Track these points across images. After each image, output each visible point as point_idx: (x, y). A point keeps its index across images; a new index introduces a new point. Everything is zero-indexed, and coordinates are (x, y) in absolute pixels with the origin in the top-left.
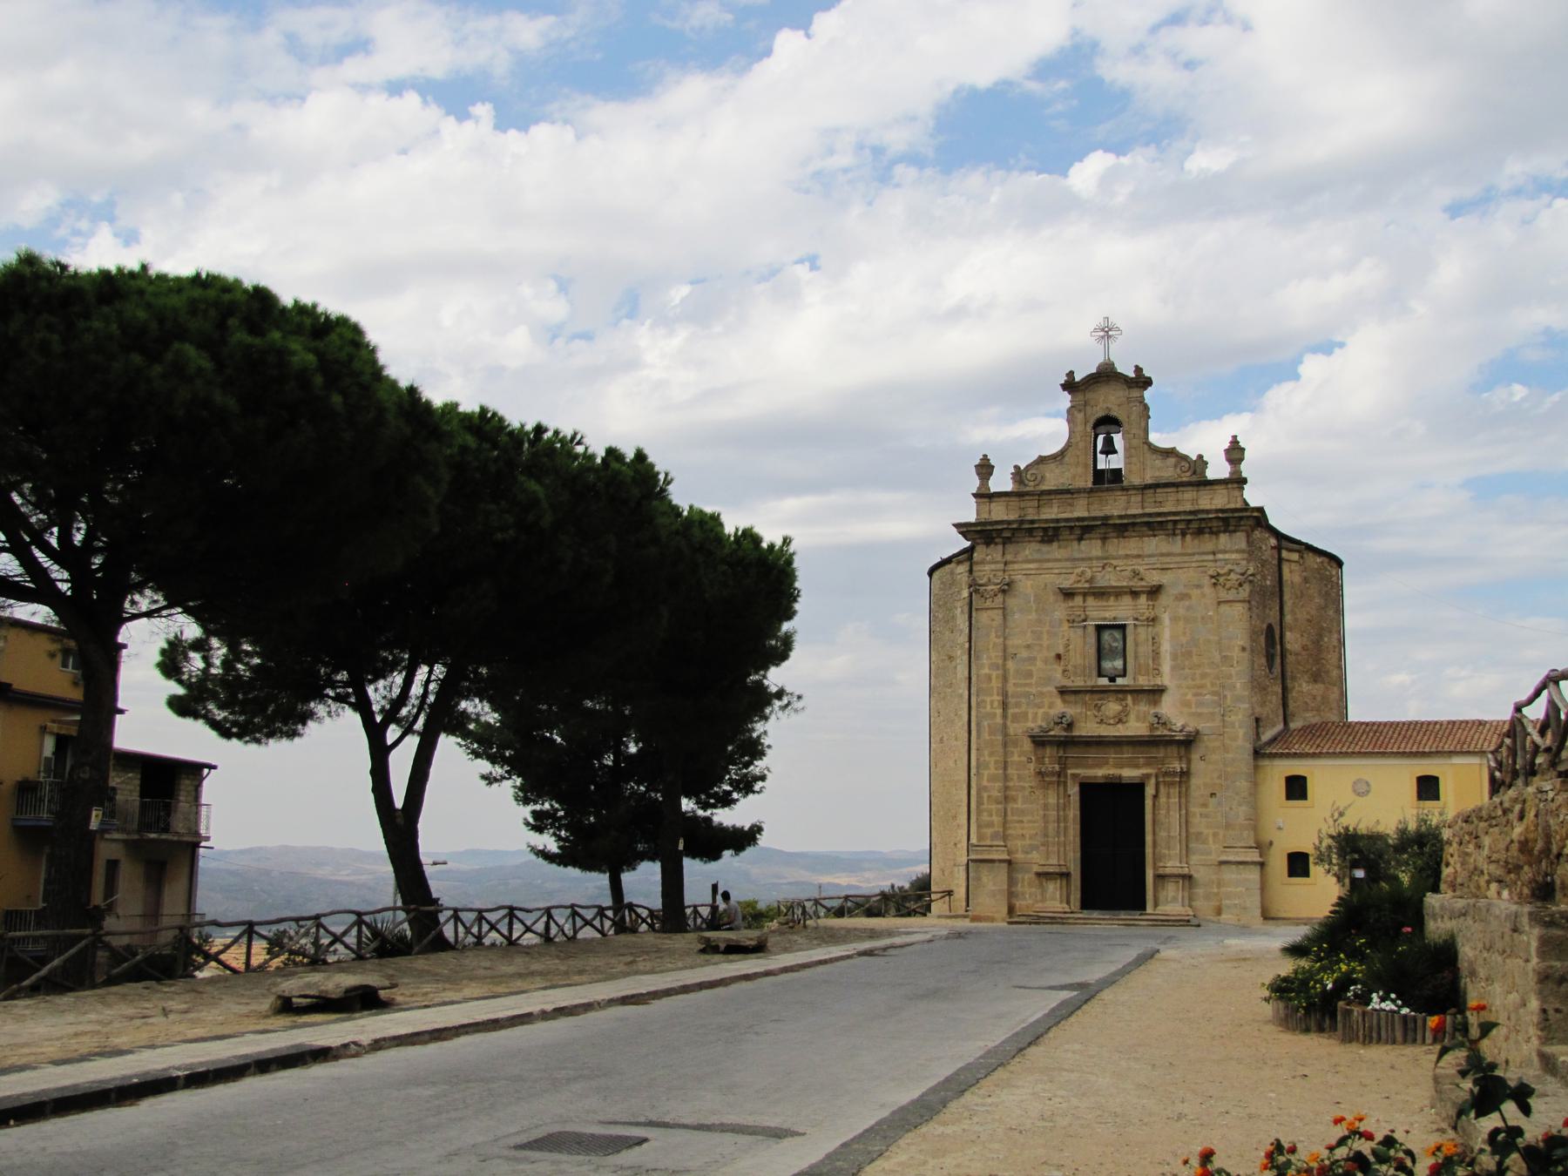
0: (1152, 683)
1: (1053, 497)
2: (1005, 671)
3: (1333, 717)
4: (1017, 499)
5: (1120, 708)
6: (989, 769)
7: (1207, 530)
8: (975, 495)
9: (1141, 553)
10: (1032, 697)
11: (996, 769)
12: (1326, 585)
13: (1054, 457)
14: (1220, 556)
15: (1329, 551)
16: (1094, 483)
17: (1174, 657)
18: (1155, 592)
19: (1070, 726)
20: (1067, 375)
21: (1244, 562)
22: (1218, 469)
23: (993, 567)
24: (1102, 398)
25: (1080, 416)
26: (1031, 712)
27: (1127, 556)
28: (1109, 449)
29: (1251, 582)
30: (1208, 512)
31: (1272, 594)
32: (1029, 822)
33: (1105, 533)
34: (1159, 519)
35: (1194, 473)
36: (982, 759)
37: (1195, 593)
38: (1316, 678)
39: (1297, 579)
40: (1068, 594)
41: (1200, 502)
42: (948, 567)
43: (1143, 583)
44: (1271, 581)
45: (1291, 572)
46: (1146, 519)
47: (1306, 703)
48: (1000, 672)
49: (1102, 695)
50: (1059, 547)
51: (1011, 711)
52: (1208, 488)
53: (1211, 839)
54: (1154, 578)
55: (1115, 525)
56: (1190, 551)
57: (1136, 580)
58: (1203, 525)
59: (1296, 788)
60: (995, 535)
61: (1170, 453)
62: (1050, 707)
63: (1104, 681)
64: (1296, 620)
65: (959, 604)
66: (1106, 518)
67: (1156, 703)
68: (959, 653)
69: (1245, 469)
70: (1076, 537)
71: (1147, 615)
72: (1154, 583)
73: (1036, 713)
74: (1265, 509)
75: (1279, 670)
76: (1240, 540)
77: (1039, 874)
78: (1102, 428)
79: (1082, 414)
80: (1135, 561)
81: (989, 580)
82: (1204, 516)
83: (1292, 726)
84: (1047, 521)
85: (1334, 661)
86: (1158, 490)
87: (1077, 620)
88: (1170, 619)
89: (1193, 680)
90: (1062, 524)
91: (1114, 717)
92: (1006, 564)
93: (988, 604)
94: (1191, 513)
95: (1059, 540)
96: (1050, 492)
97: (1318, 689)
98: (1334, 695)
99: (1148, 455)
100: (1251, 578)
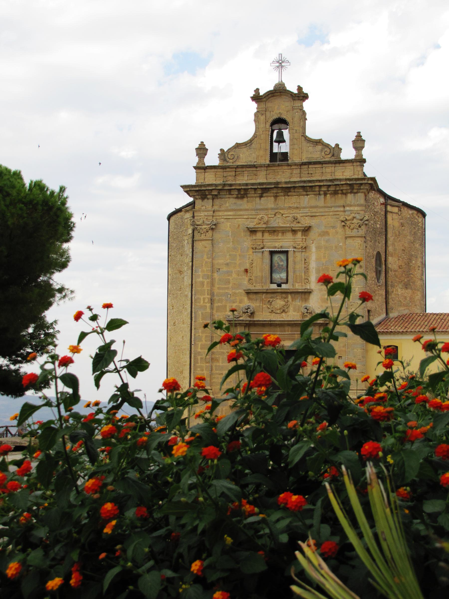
0: (304, 288)
1: (244, 170)
2: (213, 280)
3: (418, 311)
4: (221, 170)
5: (284, 303)
6: (202, 341)
7: (340, 192)
8: (194, 167)
9: (298, 206)
10: (229, 296)
11: (206, 341)
12: (414, 228)
13: (245, 144)
14: (347, 208)
15: (417, 207)
16: (271, 161)
18: (307, 230)
19: (252, 314)
20: (255, 91)
21: (362, 212)
23: (206, 213)
24: (276, 107)
25: (262, 118)
27: (290, 208)
28: (281, 140)
29: (366, 224)
30: (340, 180)
31: (380, 233)
34: (310, 184)
35: (333, 155)
36: (197, 335)
37: (332, 231)
38: (406, 286)
39: (397, 224)
40: (253, 231)
41: (337, 174)
42: (179, 214)
43: (300, 225)
44: (380, 225)
45: (392, 219)
46: (302, 184)
47: (400, 301)
48: (209, 280)
49: (273, 295)
50: (248, 202)
51: (216, 305)
52: (341, 165)
54: (306, 222)
55: (282, 188)
56: (329, 205)
57: (295, 223)
58: (338, 189)
60: (207, 193)
61: (319, 142)
62: (240, 303)
63: (274, 286)
64: (395, 250)
65: (186, 238)
66: (278, 183)
67: (306, 300)
68: (186, 269)
69: (365, 153)
70: (258, 195)
71: (301, 245)
72: (306, 225)
74: (376, 179)
75: (384, 281)
76: (360, 198)
78: (276, 126)
79: (264, 116)
80: (295, 211)
81: (204, 222)
82: (338, 183)
83: (391, 315)
84: (240, 185)
85: (419, 275)
86: (310, 166)
87: (258, 247)
90: (250, 187)
91: (280, 309)
92: (214, 212)
93: (203, 237)
94: (331, 181)
95: (247, 197)
96: (243, 167)
97: (408, 293)
98: (418, 296)
99: (305, 143)
100: (366, 222)
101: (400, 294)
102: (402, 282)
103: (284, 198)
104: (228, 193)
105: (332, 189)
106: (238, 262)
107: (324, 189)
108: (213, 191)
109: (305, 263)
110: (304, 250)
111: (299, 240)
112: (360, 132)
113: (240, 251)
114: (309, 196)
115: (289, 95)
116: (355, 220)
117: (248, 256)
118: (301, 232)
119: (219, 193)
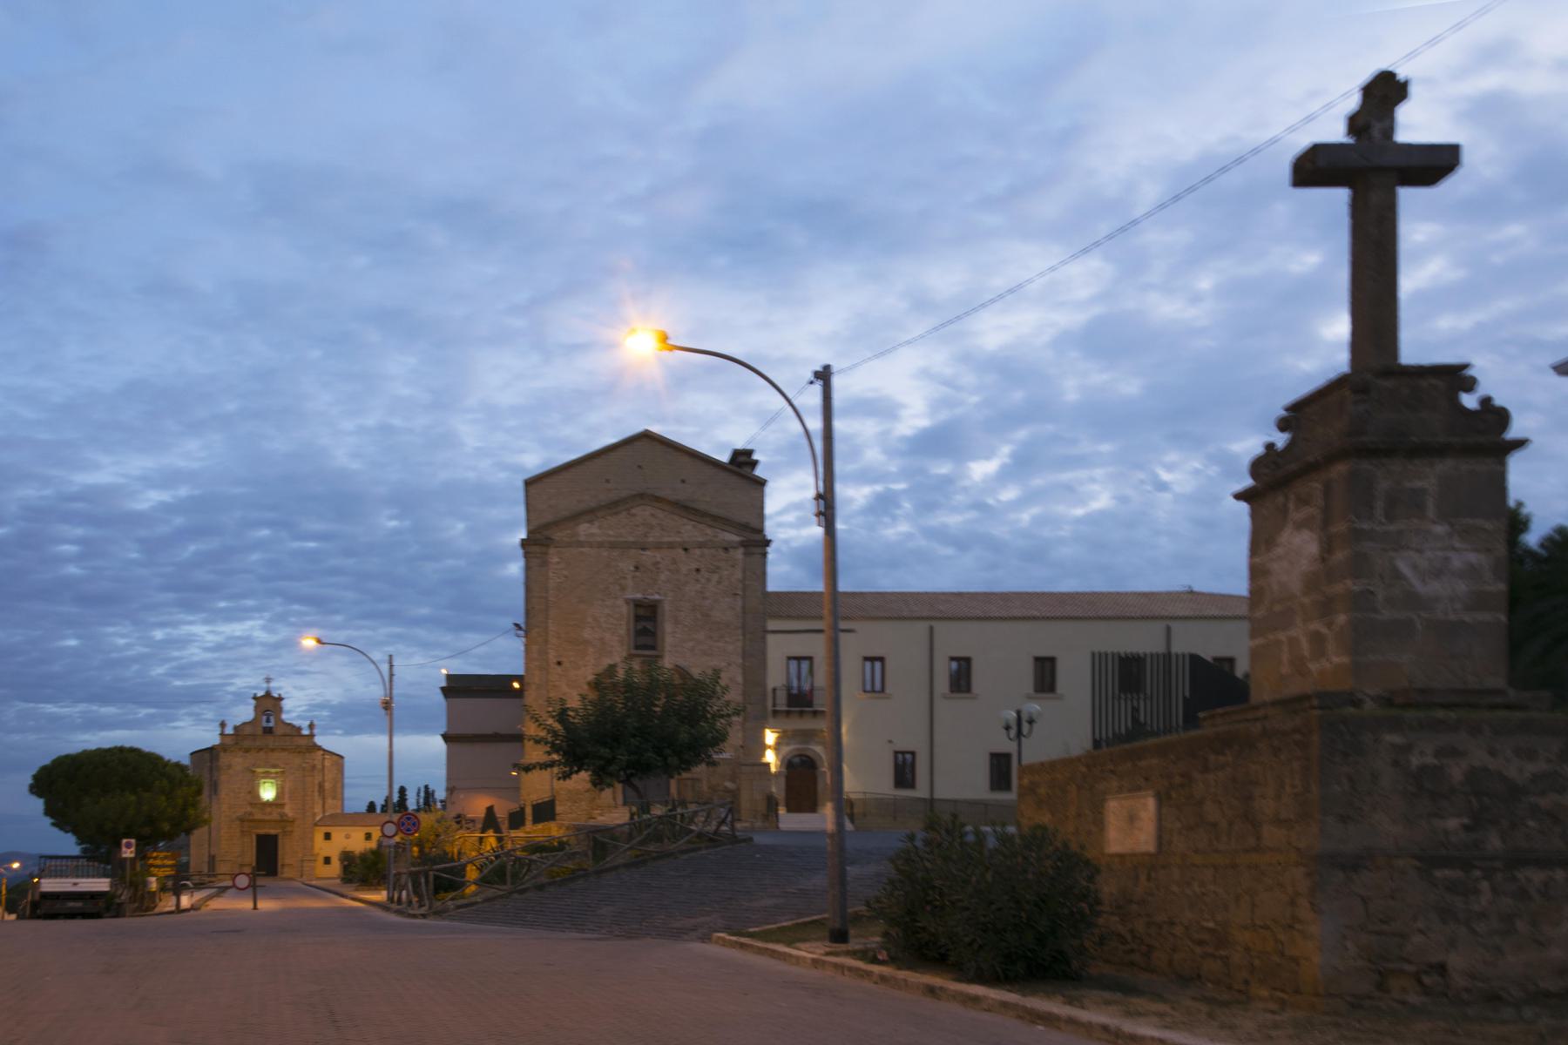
22: (306, 732)
28: (268, 721)
38: (334, 798)
59: (328, 836)
61: (289, 724)
69: (316, 731)
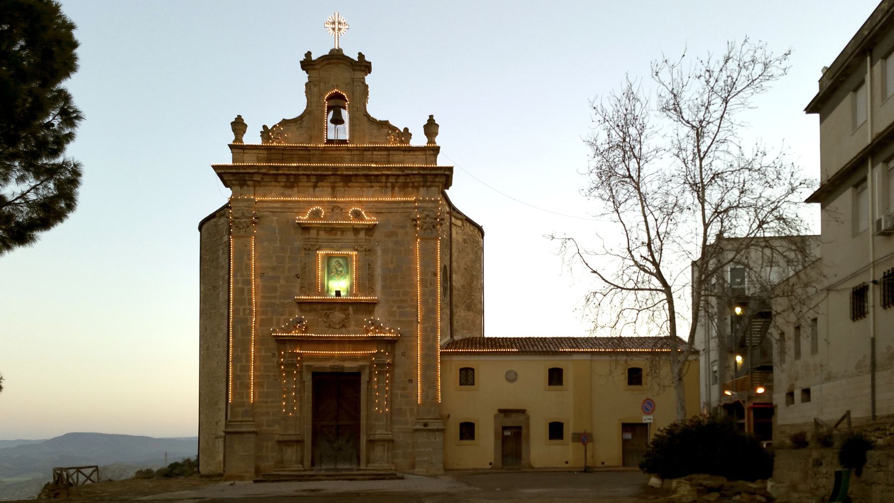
7: (410, 185)
10: (276, 307)
17: (384, 279)
22: (419, 140)
26: (275, 318)
32: (272, 402)
33: (335, 182)
34: (376, 173)
38: (469, 308)
46: (365, 172)
47: (463, 324)
49: (330, 306)
50: (299, 192)
52: (411, 153)
53: (408, 414)
58: (408, 181)
60: (247, 179)
69: (439, 141)
70: (312, 184)
71: (364, 247)
73: (280, 319)
77: (279, 442)
81: (243, 214)
88: (382, 250)
89: (398, 296)
91: (339, 323)
95: (298, 187)
99: (367, 124)
101: (462, 315)
102: (464, 303)
103: (343, 189)
104: (273, 180)
105: (401, 180)
106: (287, 266)
107: (392, 180)
108: (255, 175)
109: (369, 268)
110: (368, 253)
111: (362, 241)
112: (433, 116)
113: (289, 251)
114: (373, 189)
115: (349, 64)
116: (428, 218)
117: (299, 259)
118: (364, 232)
119: (262, 179)
